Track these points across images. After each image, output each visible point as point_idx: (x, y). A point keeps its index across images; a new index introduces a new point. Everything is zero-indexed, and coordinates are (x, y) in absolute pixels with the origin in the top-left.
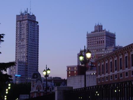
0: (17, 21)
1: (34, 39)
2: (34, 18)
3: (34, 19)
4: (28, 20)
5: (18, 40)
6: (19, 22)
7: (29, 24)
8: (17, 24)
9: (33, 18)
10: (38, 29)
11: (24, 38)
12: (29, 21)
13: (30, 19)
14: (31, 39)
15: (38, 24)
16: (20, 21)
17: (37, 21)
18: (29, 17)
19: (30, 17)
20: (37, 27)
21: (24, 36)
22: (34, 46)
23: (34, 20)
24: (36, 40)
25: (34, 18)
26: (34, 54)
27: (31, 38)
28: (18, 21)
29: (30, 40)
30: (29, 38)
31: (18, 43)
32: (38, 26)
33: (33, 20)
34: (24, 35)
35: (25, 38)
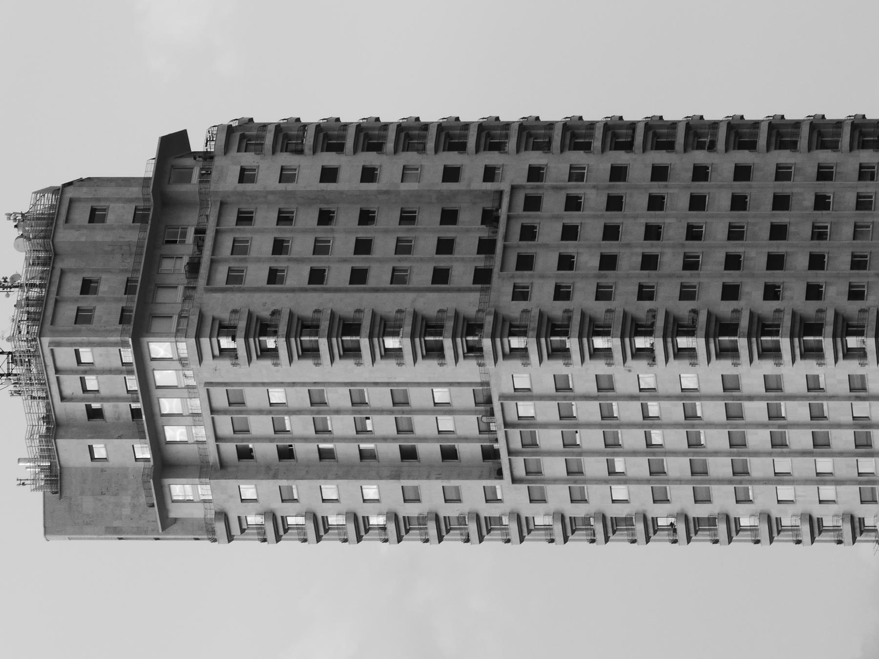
0: (167, 523)
1: (489, 218)
2: (96, 216)
3: (120, 213)
4: (138, 324)
5: (513, 496)
6: (179, 489)
7: (219, 305)
8: (221, 526)
9: (99, 235)
10: (288, 136)
11: (465, 398)
12: (171, 299)
13: (111, 285)
14: (482, 277)
15: (197, 144)
16: (165, 465)
17: (153, 150)
18: (83, 317)
19: (87, 287)
20: (268, 169)
21: (442, 389)
22: (615, 203)
23: (139, 217)
24: (490, 174)
25: (96, 216)
26: (759, 218)
27: (462, 273)
28: (162, 500)
29: (502, 287)
30: (469, 303)
31: (558, 497)
32: (241, 135)
33: (135, 236)
34: (418, 397)
35: (469, 370)
